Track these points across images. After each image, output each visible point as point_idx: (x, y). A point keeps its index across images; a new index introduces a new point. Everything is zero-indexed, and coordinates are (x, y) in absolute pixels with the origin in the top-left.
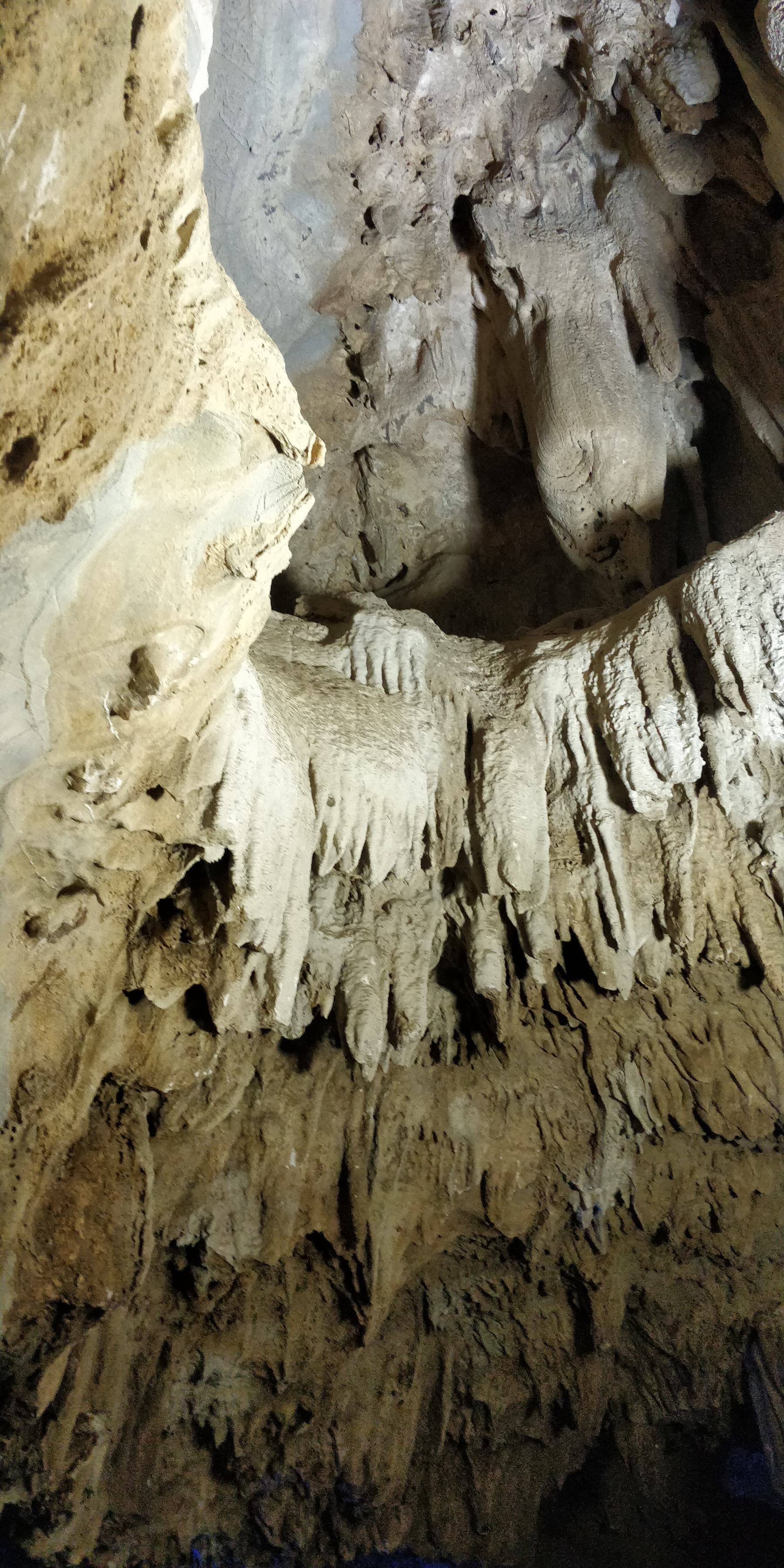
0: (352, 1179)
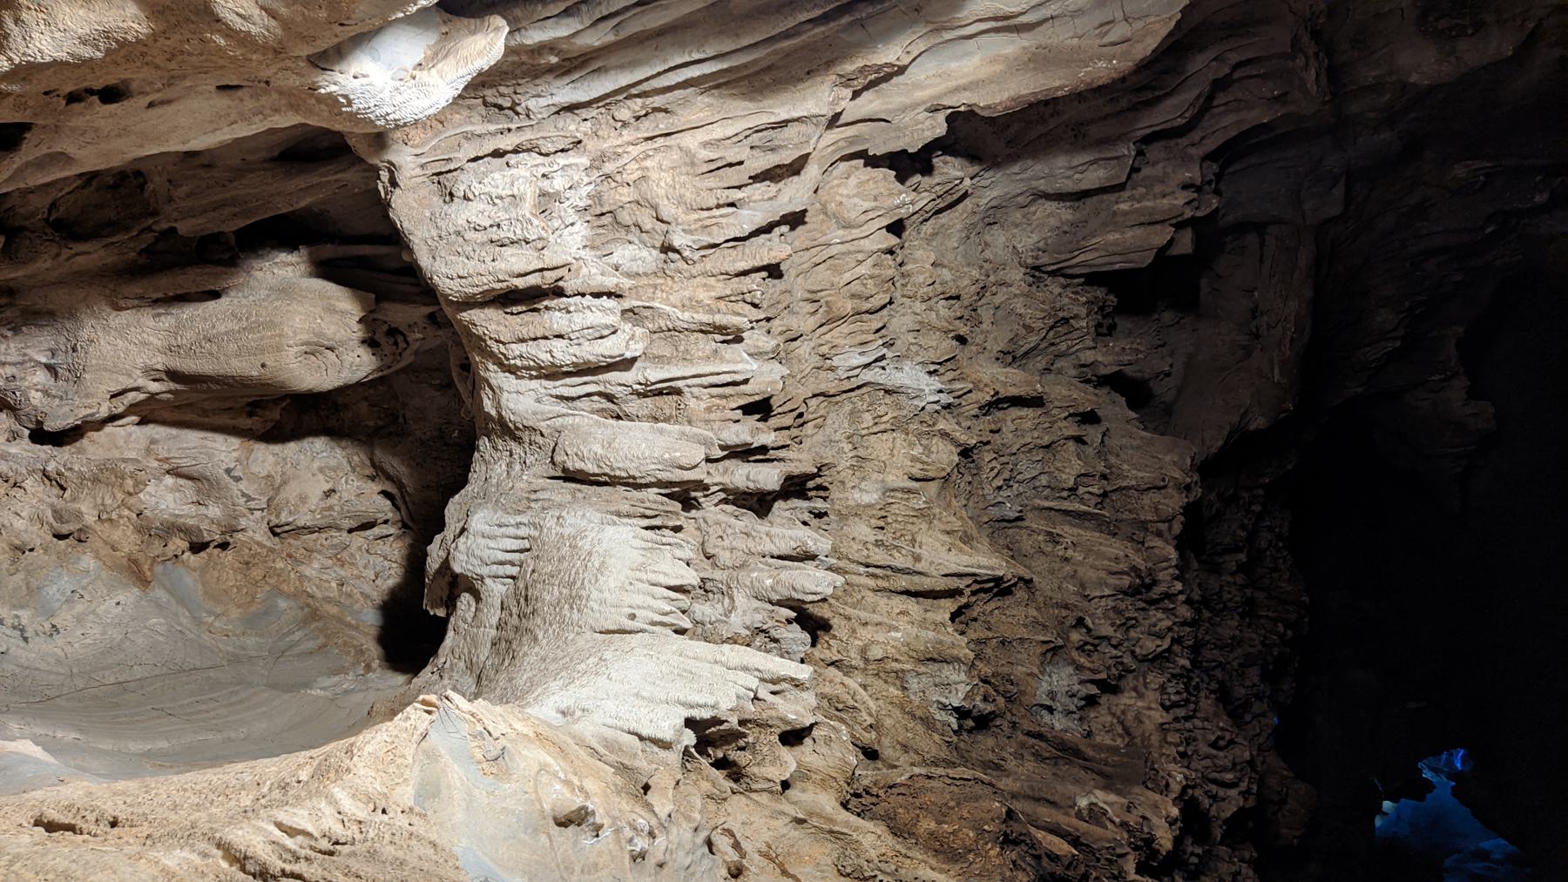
0: (912, 589)
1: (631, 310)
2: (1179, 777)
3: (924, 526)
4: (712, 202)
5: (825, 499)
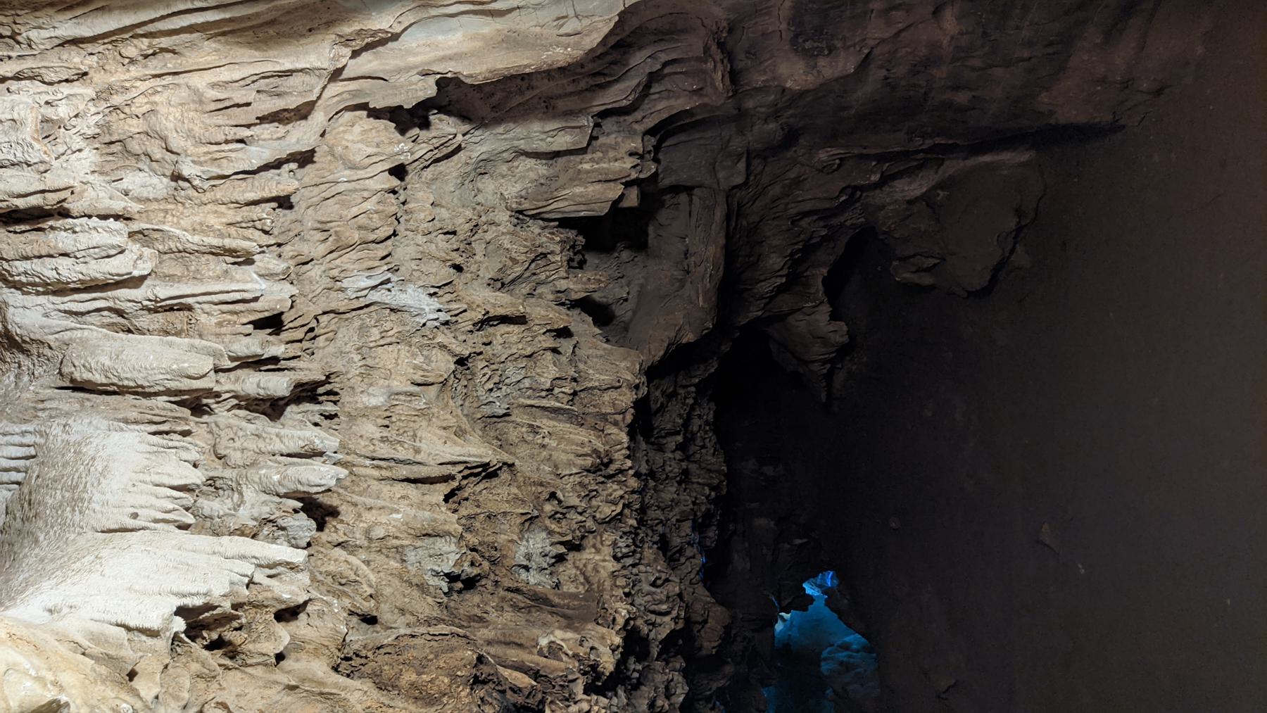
1: (140, 232)
2: (624, 612)
3: (424, 423)
4: (221, 138)
5: (335, 403)
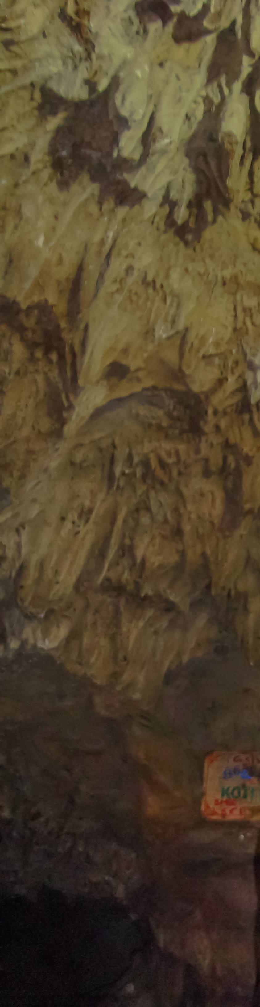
0: (85, 275)
